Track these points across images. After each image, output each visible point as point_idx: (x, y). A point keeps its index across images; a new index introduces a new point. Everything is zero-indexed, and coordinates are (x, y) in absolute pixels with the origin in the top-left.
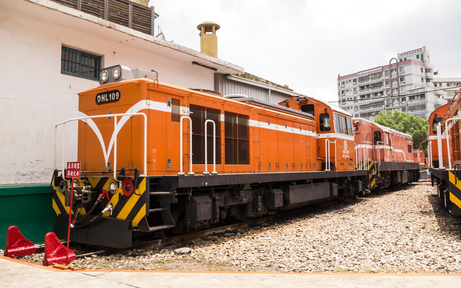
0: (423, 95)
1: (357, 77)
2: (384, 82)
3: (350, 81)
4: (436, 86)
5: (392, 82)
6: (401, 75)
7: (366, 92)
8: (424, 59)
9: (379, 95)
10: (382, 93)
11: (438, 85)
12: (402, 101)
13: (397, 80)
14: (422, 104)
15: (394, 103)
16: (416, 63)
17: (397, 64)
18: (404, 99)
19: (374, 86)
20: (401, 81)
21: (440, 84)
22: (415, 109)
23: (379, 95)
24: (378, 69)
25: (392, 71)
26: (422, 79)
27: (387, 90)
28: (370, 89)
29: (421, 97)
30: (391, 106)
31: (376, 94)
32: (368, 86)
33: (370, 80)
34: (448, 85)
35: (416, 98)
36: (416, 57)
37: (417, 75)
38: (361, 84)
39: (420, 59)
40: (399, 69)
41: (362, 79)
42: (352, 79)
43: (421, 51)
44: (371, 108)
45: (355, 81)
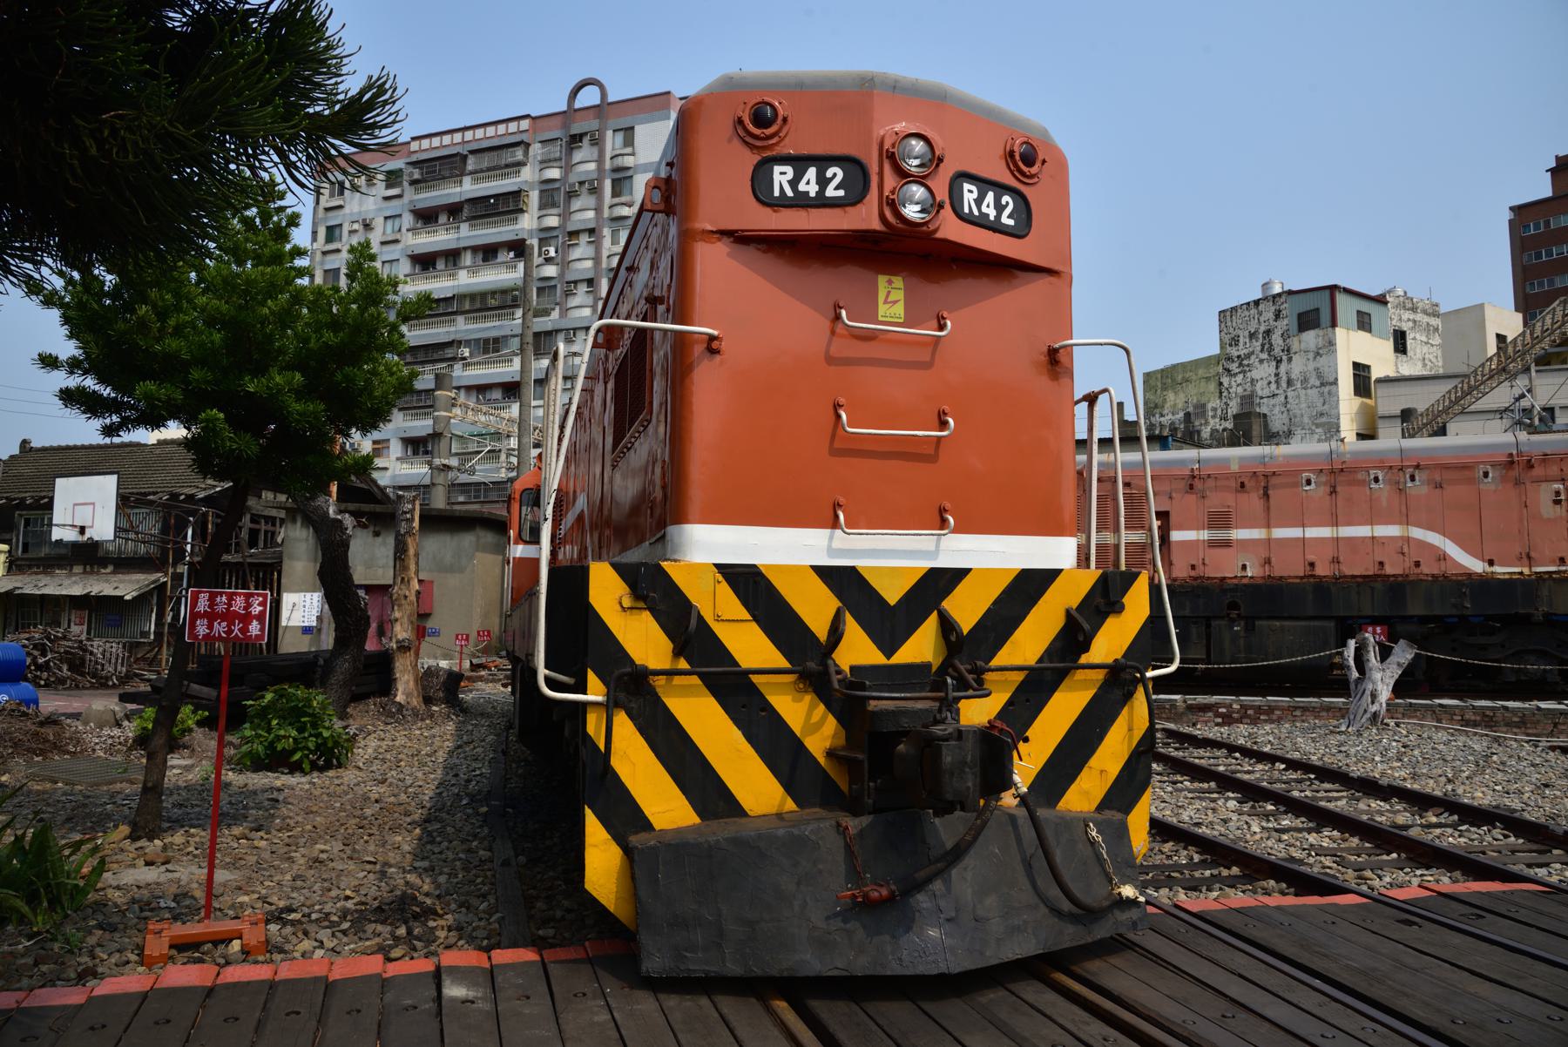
5: (571, 195)
6: (620, 162)
7: (439, 238)
9: (506, 256)
13: (595, 191)
15: (573, 302)
17: (602, 109)
20: (615, 194)
25: (575, 140)
28: (464, 227)
30: (555, 314)
31: (488, 253)
32: (454, 210)
33: (467, 180)
40: (609, 133)
44: (460, 319)
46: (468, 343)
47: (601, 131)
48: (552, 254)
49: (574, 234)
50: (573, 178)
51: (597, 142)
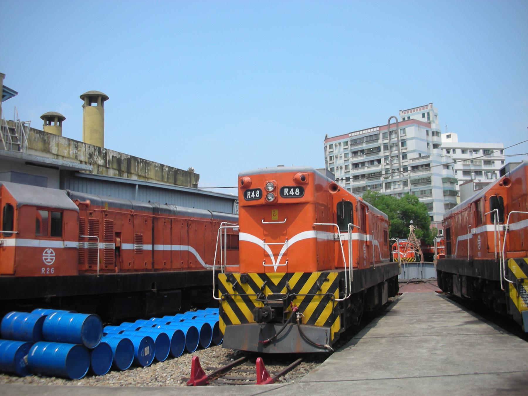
1: (348, 139)
2: (382, 148)
3: (340, 144)
5: (391, 147)
8: (431, 119)
9: (376, 163)
10: (379, 161)
11: (451, 151)
14: (427, 176)
16: (419, 123)
17: (397, 124)
19: (370, 151)
20: (403, 145)
21: (454, 150)
22: (419, 183)
24: (375, 129)
25: (391, 133)
26: (428, 144)
27: (386, 158)
30: (390, 178)
31: (372, 162)
32: (362, 151)
35: (420, 168)
36: (421, 115)
37: (422, 140)
38: (353, 148)
39: (425, 120)
40: (399, 130)
41: (355, 142)
42: (342, 141)
43: (427, 108)
45: (346, 143)
46: (369, 186)
47: (397, 130)
50: (391, 143)
51: (397, 133)
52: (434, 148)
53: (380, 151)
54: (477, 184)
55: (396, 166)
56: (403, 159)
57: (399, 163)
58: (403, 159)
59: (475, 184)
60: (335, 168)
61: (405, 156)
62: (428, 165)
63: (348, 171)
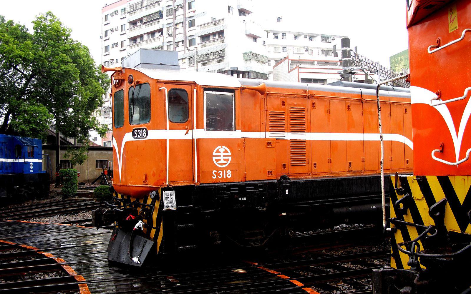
0: (221, 33)
4: (277, 37)
5: (176, 10)
9: (157, 34)
12: (190, 45)
14: (219, 49)
18: (191, 43)
20: (190, 8)
21: (284, 35)
23: (157, 34)
29: (219, 37)
31: (153, 33)
32: (141, 20)
33: (144, 9)
34: (296, 37)
35: (211, 38)
48: (170, 33)
49: (176, 25)
52: (240, 14)
53: (161, 16)
54: (293, 62)
55: (180, 38)
56: (190, 26)
57: (185, 33)
58: (190, 26)
59: (290, 62)
60: (111, 46)
61: (192, 24)
62: (221, 33)
63: (123, 48)
